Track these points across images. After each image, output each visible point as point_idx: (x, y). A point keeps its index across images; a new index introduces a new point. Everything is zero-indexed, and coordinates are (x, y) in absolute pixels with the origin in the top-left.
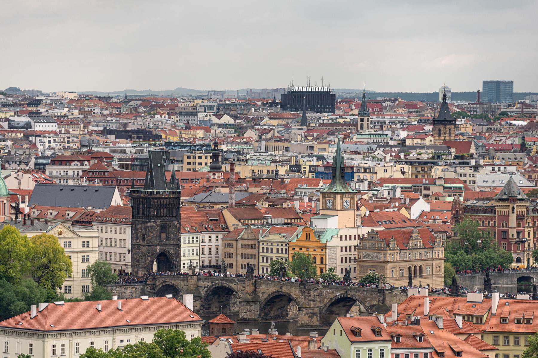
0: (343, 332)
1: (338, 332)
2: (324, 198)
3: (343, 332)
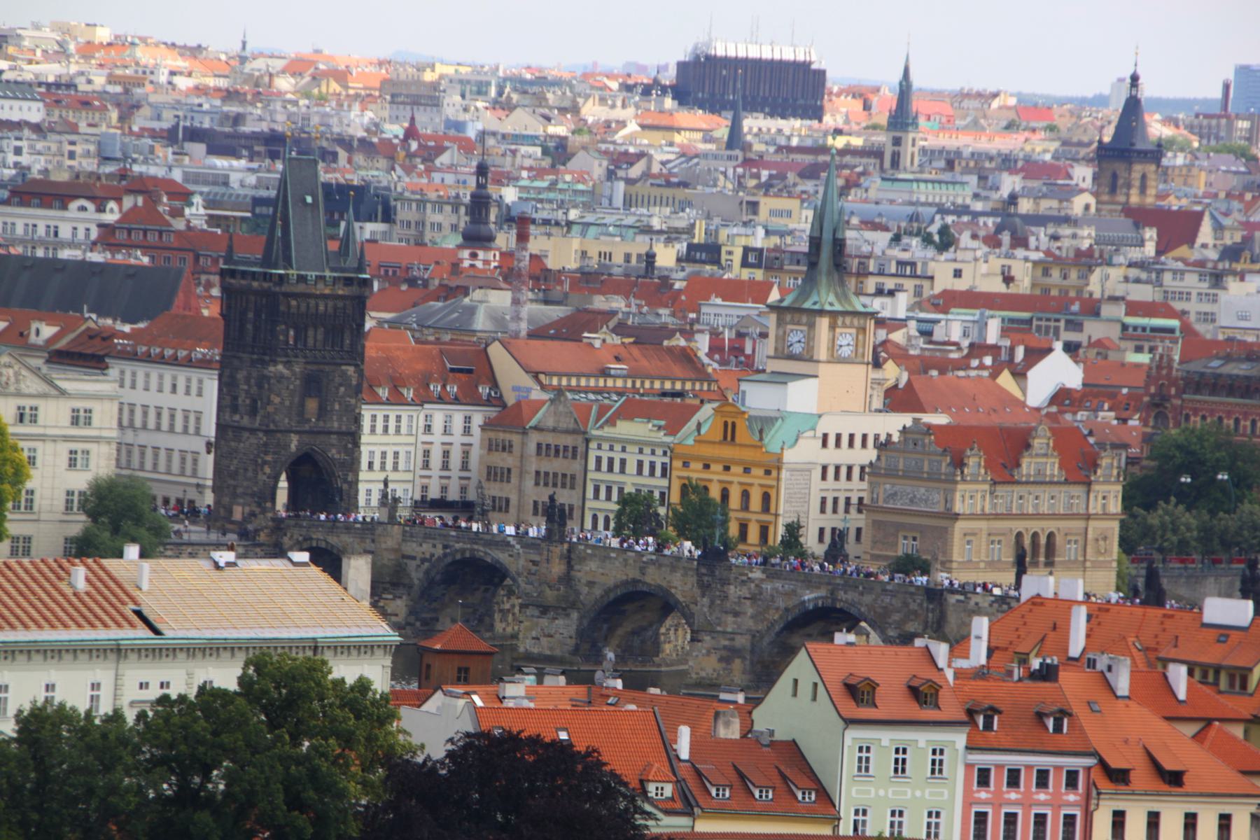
0: (821, 688)
1: (805, 689)
2: (780, 323)
3: (821, 688)
